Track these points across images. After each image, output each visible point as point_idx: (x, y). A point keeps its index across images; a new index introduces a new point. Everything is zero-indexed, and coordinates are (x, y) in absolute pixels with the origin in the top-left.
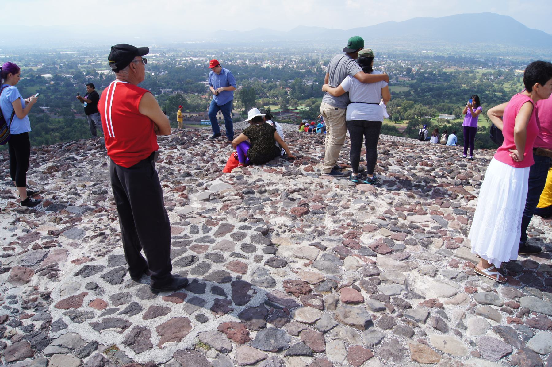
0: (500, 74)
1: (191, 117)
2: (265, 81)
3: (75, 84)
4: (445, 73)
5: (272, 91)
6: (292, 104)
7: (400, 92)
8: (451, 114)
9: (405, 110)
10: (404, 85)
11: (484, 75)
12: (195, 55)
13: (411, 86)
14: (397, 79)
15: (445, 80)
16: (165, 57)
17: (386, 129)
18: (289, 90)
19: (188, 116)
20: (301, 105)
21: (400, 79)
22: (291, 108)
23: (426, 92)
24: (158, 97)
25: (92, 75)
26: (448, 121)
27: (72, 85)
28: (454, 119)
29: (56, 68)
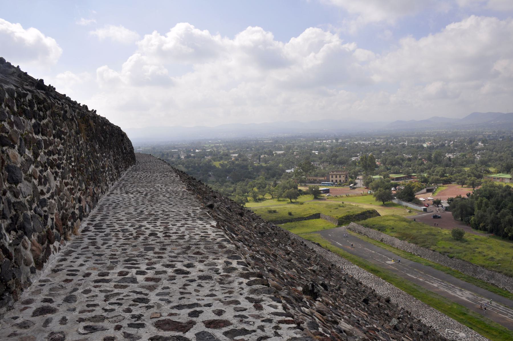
12: (361, 139)
16: (338, 142)
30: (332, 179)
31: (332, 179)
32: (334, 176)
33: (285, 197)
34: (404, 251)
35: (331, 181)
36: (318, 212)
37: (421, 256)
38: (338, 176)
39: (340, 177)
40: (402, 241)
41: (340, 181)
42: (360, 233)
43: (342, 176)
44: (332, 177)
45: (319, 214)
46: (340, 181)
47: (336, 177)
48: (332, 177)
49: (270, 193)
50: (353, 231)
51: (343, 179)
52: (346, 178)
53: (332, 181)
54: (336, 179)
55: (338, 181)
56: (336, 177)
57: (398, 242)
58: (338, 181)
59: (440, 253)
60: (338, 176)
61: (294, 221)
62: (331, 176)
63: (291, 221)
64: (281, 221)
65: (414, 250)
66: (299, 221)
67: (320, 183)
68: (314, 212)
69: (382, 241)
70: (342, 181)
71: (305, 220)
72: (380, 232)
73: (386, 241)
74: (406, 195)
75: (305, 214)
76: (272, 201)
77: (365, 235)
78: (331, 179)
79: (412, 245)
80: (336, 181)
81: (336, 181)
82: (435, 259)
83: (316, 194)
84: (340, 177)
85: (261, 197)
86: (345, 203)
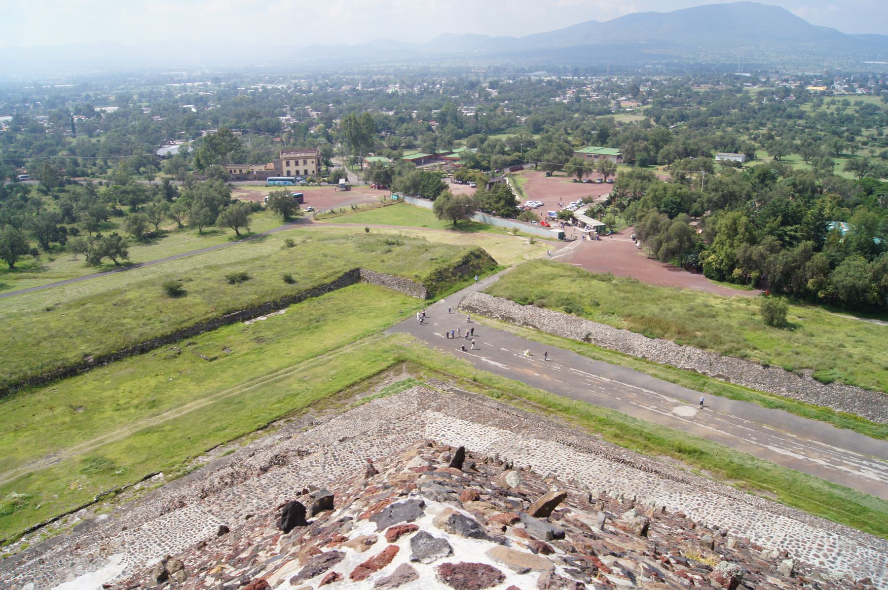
0: (787, 91)
1: (249, 173)
2: (391, 113)
3: (48, 128)
4: (697, 93)
5: (405, 125)
6: (443, 144)
7: (631, 122)
8: (736, 152)
9: (658, 147)
10: (633, 113)
11: (761, 94)
13: (647, 113)
14: (618, 103)
15: (700, 103)
16: (220, 86)
17: (638, 178)
18: (435, 125)
19: (244, 171)
20: (460, 145)
21: (623, 105)
22: (441, 152)
23: (677, 121)
24: (194, 143)
25: (84, 115)
26: (738, 165)
27: (41, 130)
28: (746, 161)
29: (28, 108)
30: (288, 168)
31: (288, 168)
32: (292, 163)
33: (223, 225)
34: (669, 367)
35: (285, 173)
36: (353, 267)
37: (727, 379)
38: (301, 162)
39: (305, 163)
40: (657, 341)
41: (306, 172)
42: (507, 319)
43: (309, 161)
44: (288, 164)
45: (358, 270)
46: (306, 172)
47: (297, 164)
48: (288, 164)
49: (172, 217)
50: (484, 314)
51: (311, 167)
52: (319, 164)
53: (289, 173)
54: (297, 168)
55: (302, 173)
56: (297, 164)
57: (640, 342)
58: (302, 173)
59: (788, 370)
60: (301, 162)
61: (306, 298)
62: (284, 163)
63: (297, 299)
64: (275, 303)
65: (700, 361)
66: (317, 295)
67: (265, 179)
68: (342, 267)
69: (587, 339)
70: (310, 172)
71: (330, 290)
72: (573, 316)
73: (602, 341)
74: (502, 203)
75: (324, 274)
76: (181, 236)
77: (526, 324)
78: (285, 169)
79: (690, 350)
80: (297, 172)
81: (297, 172)
82: (773, 385)
83: (288, 209)
84: (305, 163)
85: (152, 229)
86: (374, 231)
